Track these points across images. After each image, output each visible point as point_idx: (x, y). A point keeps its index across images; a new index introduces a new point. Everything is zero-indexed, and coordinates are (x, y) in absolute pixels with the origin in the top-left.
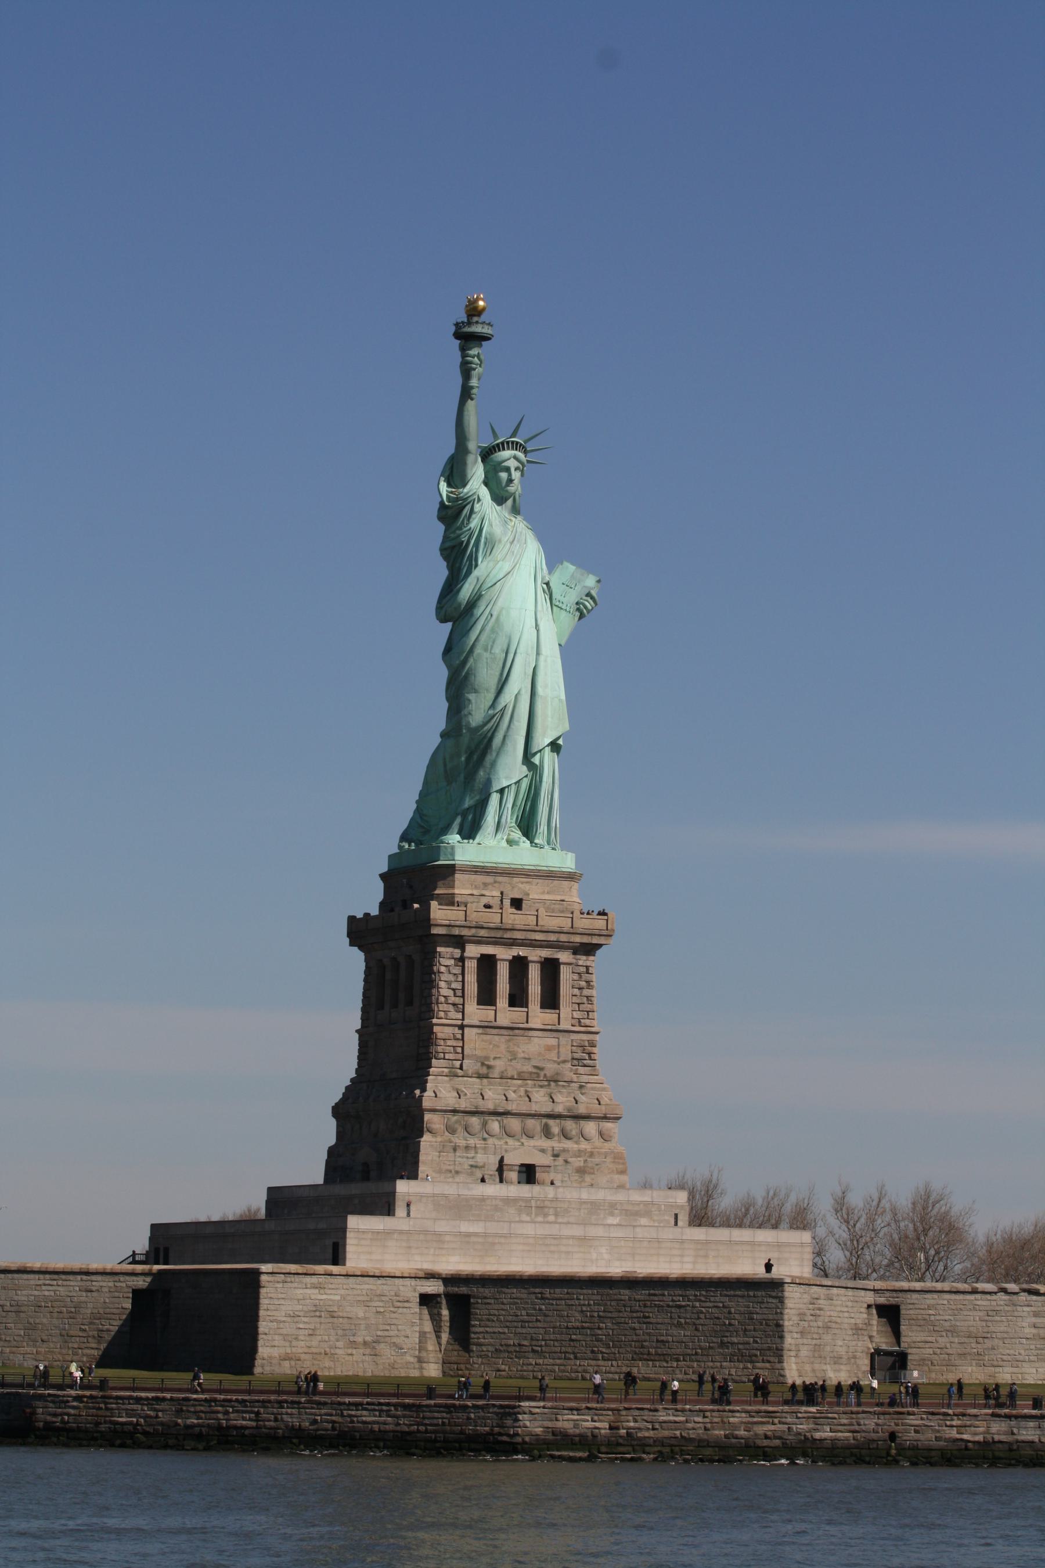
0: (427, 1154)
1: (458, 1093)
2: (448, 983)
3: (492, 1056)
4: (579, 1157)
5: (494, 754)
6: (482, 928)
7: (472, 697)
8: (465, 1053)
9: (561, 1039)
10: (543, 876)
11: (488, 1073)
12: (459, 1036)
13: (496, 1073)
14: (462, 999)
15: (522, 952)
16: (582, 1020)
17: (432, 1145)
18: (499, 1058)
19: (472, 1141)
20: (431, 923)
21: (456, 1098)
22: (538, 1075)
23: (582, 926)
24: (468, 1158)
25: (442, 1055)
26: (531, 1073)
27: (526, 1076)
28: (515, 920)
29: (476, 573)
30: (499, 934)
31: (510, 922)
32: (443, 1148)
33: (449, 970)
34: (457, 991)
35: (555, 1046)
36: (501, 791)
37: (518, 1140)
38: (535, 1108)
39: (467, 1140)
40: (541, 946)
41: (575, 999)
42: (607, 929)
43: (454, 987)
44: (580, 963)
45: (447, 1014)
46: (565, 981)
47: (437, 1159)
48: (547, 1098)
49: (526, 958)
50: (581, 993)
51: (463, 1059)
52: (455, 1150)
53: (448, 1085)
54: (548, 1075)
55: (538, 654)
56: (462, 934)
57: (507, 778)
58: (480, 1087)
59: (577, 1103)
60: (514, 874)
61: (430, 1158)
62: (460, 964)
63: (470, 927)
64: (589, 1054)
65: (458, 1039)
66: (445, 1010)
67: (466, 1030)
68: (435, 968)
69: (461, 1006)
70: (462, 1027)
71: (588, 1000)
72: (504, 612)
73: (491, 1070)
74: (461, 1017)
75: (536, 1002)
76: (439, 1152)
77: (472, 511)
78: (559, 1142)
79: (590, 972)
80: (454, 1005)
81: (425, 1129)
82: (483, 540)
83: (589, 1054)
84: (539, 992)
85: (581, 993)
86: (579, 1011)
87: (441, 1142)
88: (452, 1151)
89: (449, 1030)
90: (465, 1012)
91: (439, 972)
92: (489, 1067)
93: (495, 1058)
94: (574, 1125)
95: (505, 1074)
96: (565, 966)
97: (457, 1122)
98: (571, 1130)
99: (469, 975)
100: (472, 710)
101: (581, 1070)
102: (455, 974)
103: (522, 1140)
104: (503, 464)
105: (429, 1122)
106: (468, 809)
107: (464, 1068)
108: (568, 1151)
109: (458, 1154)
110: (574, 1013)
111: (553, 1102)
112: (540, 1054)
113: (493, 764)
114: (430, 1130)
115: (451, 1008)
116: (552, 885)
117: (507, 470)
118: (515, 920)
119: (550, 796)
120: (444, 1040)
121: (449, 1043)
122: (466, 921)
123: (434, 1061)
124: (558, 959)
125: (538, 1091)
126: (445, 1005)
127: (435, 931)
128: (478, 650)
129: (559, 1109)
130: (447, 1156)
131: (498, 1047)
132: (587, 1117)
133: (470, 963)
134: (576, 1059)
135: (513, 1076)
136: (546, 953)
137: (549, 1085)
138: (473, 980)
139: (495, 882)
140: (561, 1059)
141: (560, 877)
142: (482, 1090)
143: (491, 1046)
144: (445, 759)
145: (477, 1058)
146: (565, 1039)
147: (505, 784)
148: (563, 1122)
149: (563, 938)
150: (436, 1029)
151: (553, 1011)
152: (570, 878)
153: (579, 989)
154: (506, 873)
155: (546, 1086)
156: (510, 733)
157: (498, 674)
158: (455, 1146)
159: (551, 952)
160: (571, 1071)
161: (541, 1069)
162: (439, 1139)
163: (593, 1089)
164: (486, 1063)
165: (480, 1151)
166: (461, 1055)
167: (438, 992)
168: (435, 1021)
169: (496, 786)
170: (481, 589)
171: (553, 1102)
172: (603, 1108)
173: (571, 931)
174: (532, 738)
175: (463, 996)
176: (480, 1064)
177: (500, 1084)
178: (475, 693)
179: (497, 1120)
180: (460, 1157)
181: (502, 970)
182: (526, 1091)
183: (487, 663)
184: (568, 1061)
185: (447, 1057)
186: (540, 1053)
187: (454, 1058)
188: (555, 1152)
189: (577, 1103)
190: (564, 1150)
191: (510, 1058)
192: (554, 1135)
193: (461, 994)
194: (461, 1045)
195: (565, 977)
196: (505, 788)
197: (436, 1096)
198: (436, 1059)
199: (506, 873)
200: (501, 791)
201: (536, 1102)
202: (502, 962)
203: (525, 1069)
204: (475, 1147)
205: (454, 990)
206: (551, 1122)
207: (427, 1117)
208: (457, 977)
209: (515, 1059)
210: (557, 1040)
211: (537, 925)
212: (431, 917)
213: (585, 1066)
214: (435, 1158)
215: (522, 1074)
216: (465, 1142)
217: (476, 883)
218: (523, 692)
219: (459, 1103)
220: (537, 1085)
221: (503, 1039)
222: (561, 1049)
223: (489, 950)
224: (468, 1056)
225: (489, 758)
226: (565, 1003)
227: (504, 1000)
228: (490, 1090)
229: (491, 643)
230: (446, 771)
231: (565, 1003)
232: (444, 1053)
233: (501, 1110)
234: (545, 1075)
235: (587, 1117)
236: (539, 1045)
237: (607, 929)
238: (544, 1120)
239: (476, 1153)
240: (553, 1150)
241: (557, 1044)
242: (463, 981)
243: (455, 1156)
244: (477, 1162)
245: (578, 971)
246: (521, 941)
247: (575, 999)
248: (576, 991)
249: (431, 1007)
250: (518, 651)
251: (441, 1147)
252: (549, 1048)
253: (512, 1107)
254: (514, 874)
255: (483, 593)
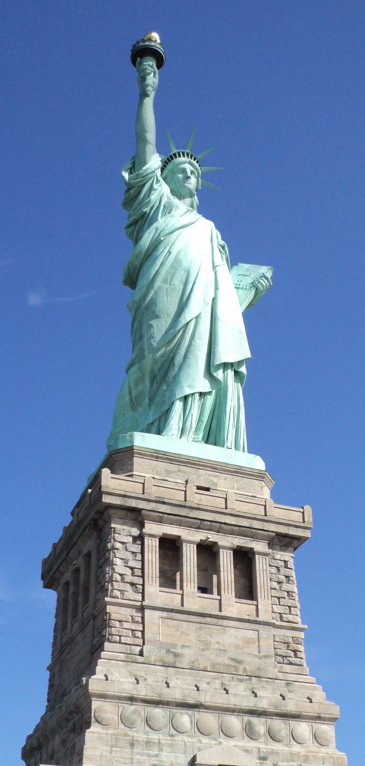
0: (93, 748)
1: (136, 679)
2: (125, 561)
3: (180, 644)
4: (293, 761)
5: (176, 369)
6: (164, 503)
7: (153, 322)
8: (146, 638)
9: (261, 632)
10: (232, 472)
11: (175, 662)
12: (140, 620)
13: (185, 663)
14: (141, 579)
15: (213, 537)
16: (283, 615)
17: (101, 738)
18: (189, 646)
19: (154, 736)
20: (103, 489)
21: (133, 683)
22: (237, 669)
23: (276, 515)
24: (149, 755)
25: (117, 638)
26: (228, 666)
27: (222, 669)
28: (201, 500)
29: (155, 225)
30: (183, 512)
31: (196, 502)
32: (116, 742)
33: (126, 548)
34: (135, 570)
35: (254, 639)
36: (185, 398)
37: (216, 739)
38: (233, 701)
39: (148, 735)
40: (232, 533)
41: (274, 593)
42: (304, 522)
43: (132, 566)
44: (278, 557)
45: (123, 594)
46: (261, 572)
47: (109, 755)
48: (249, 693)
49: (216, 543)
50: (280, 588)
51: (144, 643)
52: (132, 745)
53: (124, 670)
54: (248, 669)
55: (216, 288)
56: (140, 507)
57: (190, 387)
58: (165, 675)
59: (284, 699)
60: (199, 465)
61: (98, 753)
62: (139, 542)
63: (148, 500)
64: (295, 651)
65: (137, 622)
66: (121, 589)
67: (147, 612)
68: (109, 545)
69: (141, 587)
70: (142, 609)
71: (289, 595)
72: (182, 252)
73: (178, 659)
74: (140, 599)
75: (230, 590)
76: (112, 747)
77: (151, 188)
78: (266, 743)
79: (289, 566)
80: (132, 584)
81: (93, 719)
82: (162, 208)
83: (295, 651)
84: (233, 580)
85: (280, 588)
86: (280, 605)
87: (113, 734)
88: (128, 746)
89: (126, 613)
90: (146, 593)
91: (114, 548)
92: (176, 655)
93: (183, 646)
94: (283, 725)
95: (196, 665)
96: (261, 556)
97: (135, 712)
98: (280, 731)
99: (150, 554)
100: (153, 333)
101: (287, 668)
102: (133, 553)
103: (220, 740)
104: (180, 167)
105: (99, 709)
106: (152, 424)
107: (145, 654)
108: (278, 753)
109: (135, 750)
110: (275, 607)
111: (256, 696)
112: (237, 647)
113: (176, 377)
114: (99, 720)
115: (128, 587)
116: (242, 482)
117: (184, 171)
118: (201, 500)
119: (236, 419)
120: (120, 621)
121: (126, 625)
122: (143, 493)
123: (106, 644)
124: (252, 549)
125: (237, 685)
126: (122, 584)
127: (106, 499)
128: (158, 283)
129: (264, 704)
130: (121, 751)
131: (187, 634)
132: (296, 717)
133: (150, 541)
134: (280, 656)
135: (206, 667)
136: (238, 541)
137: (250, 680)
138: (154, 560)
139: (179, 471)
140: (263, 653)
141: (250, 475)
142: (167, 678)
143: (179, 633)
144: (130, 387)
145: (161, 645)
146: (265, 632)
147: (188, 391)
148: (269, 721)
149: (256, 524)
150: (109, 609)
151: (250, 602)
152: (260, 477)
153: (279, 583)
154: (190, 463)
155: (246, 680)
156: (192, 348)
157: (177, 301)
158: (133, 740)
159: (244, 541)
160: (275, 667)
161: (240, 662)
162: (111, 731)
163: (302, 687)
164: (173, 650)
165: (165, 748)
166: (142, 640)
167: (113, 569)
168: (107, 599)
169: (180, 394)
170: (161, 235)
171: (256, 696)
172: (316, 706)
173: (265, 518)
174: (214, 353)
175: (143, 577)
176: (165, 650)
177: (190, 674)
178: (156, 318)
179: (187, 713)
180: (138, 753)
181: (188, 553)
182: (223, 684)
183: (167, 292)
184: (272, 657)
185: (123, 640)
186: (238, 645)
187: (132, 643)
188: (262, 755)
189: (284, 699)
190: (273, 752)
191: (201, 648)
192: (259, 735)
193: (140, 574)
194: (141, 629)
195: (261, 567)
196: (189, 395)
197: (107, 679)
198: (109, 641)
199: (190, 463)
200: (185, 398)
201: (235, 695)
202: (188, 545)
203: (220, 660)
204: (159, 743)
205: (132, 569)
206: (255, 720)
207: (95, 704)
208: (136, 556)
209: (208, 649)
210: (257, 632)
211: (226, 508)
212: (102, 484)
213: (291, 664)
214: (105, 754)
215: (216, 666)
216: (146, 736)
217: (158, 469)
218: (203, 316)
219: (137, 690)
220: (235, 679)
221: (193, 626)
222: (261, 643)
223: (173, 531)
224: (150, 641)
225: (172, 373)
226: (263, 594)
227: (192, 584)
228: (177, 679)
229: (170, 277)
230: (131, 400)
231: (263, 594)
232: (120, 636)
233: (192, 701)
234: (245, 670)
235: (296, 717)
236: (237, 638)
237: (304, 522)
238: (247, 718)
239: (161, 750)
240: (259, 751)
241: (257, 637)
242: (143, 561)
243: (132, 752)
244: (162, 761)
245: (276, 565)
246: (209, 523)
247: (274, 593)
248: (275, 585)
249: (104, 586)
250: (197, 281)
251: (114, 741)
252: (248, 641)
253: (205, 699)
254: (199, 465)
255: (162, 239)
